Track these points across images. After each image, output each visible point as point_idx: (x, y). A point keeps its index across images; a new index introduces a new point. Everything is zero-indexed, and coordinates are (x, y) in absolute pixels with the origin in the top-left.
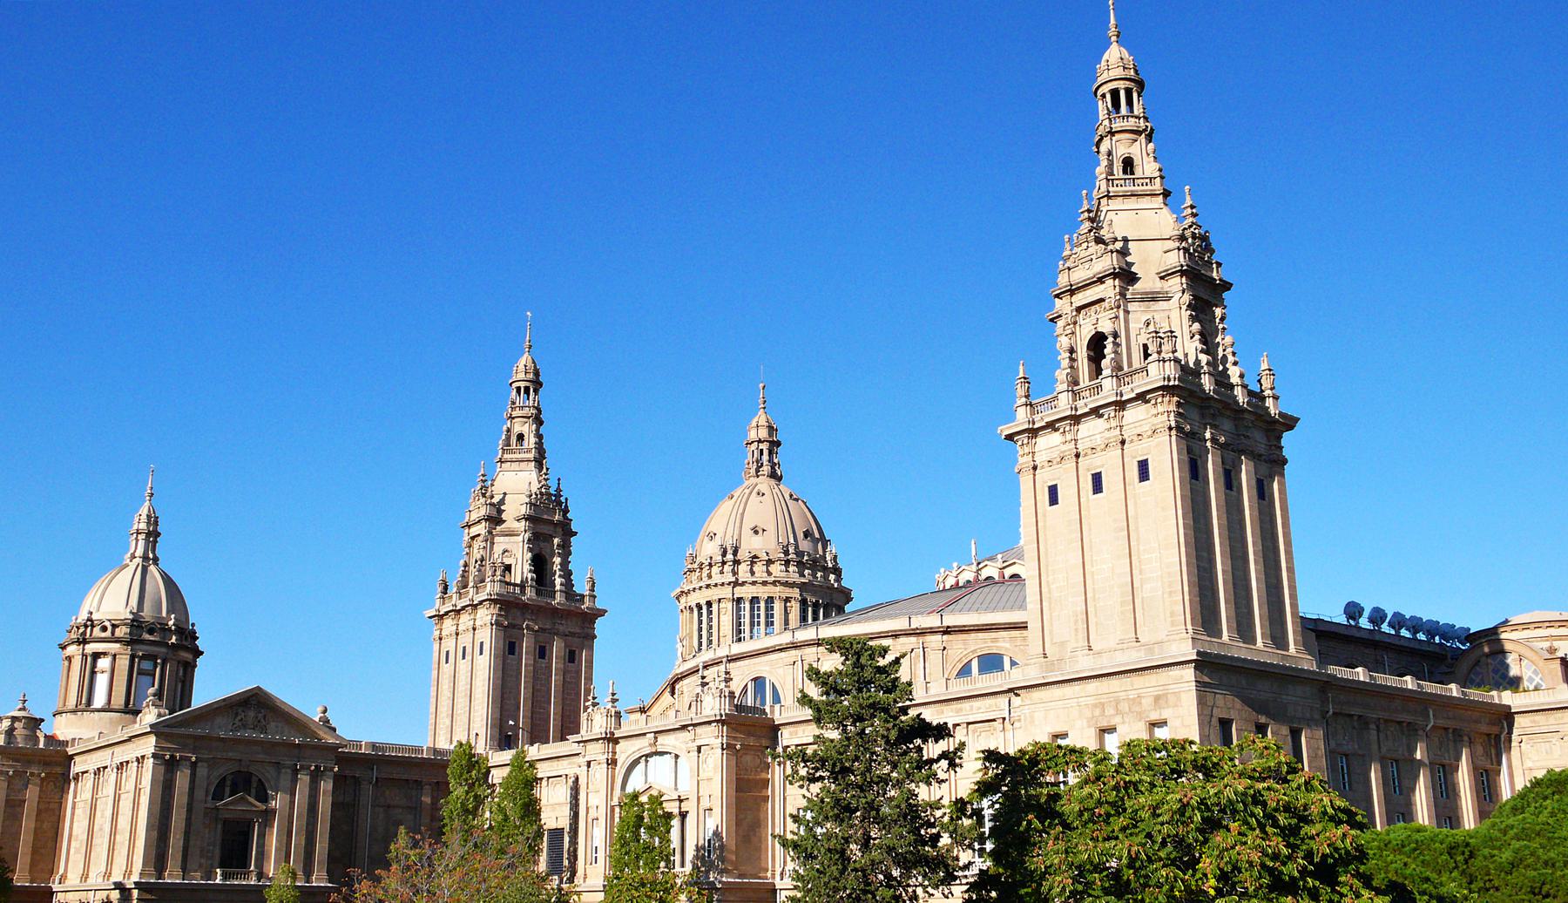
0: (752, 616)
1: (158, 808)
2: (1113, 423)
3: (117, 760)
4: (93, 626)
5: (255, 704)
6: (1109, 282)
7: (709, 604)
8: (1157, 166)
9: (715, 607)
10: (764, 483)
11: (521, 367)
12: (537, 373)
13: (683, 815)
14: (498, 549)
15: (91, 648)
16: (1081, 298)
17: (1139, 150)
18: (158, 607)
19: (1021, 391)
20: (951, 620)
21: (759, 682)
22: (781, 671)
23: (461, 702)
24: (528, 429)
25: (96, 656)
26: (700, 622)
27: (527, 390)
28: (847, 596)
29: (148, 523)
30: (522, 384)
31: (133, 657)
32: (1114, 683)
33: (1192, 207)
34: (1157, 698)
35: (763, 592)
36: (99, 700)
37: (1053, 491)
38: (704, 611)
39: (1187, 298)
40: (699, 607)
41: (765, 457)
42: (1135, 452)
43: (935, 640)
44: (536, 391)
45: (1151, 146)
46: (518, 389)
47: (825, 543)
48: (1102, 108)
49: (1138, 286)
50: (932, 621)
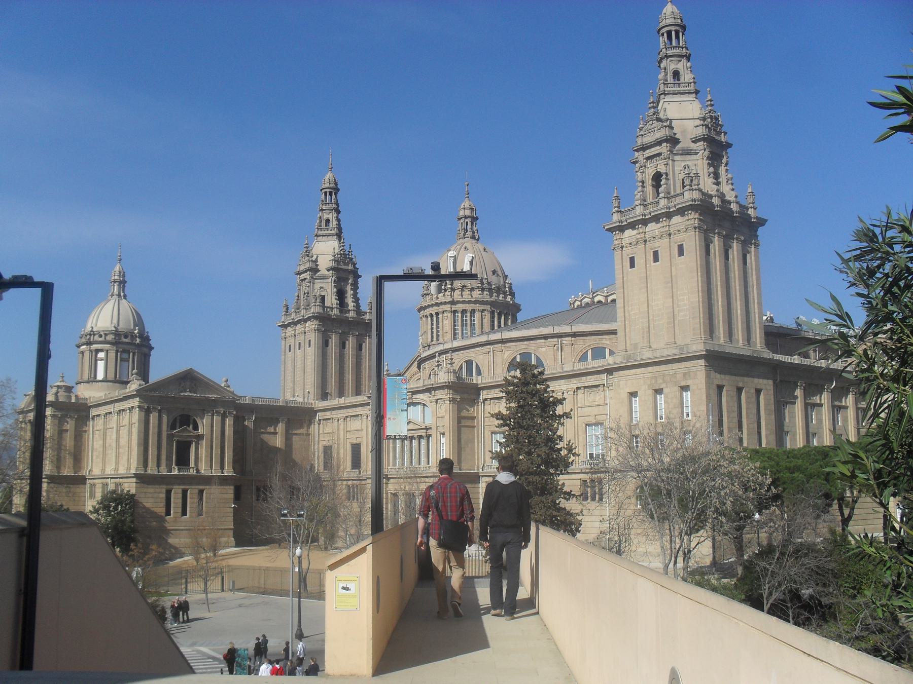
0: (462, 321)
1: (142, 435)
2: (665, 224)
3: (117, 409)
4: (94, 335)
5: (189, 378)
6: (664, 144)
7: (437, 314)
8: (692, 76)
9: (441, 316)
10: (468, 243)
11: (327, 180)
12: (336, 184)
13: (428, 437)
14: (317, 286)
15: (95, 346)
16: (648, 153)
17: (682, 66)
18: (128, 323)
19: (615, 204)
20: (576, 328)
21: (469, 363)
22: (481, 357)
23: (299, 373)
24: (332, 216)
25: (97, 351)
26: (432, 324)
27: (331, 194)
28: (517, 308)
29: (120, 276)
30: (328, 190)
31: (117, 352)
32: (663, 367)
33: (711, 100)
34: (685, 374)
35: (469, 307)
36: (100, 376)
37: (632, 260)
38: (434, 318)
39: (707, 153)
40: (431, 315)
41: (469, 226)
42: (678, 238)
43: (566, 340)
44: (336, 194)
45: (689, 64)
46: (326, 193)
47: (506, 277)
48: (663, 40)
49: (679, 147)
50: (566, 329)
